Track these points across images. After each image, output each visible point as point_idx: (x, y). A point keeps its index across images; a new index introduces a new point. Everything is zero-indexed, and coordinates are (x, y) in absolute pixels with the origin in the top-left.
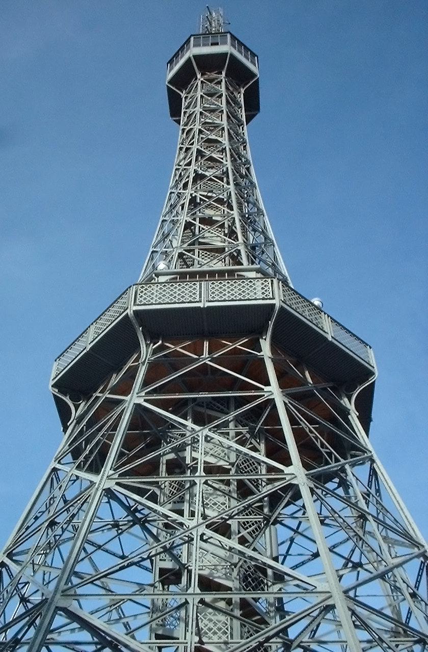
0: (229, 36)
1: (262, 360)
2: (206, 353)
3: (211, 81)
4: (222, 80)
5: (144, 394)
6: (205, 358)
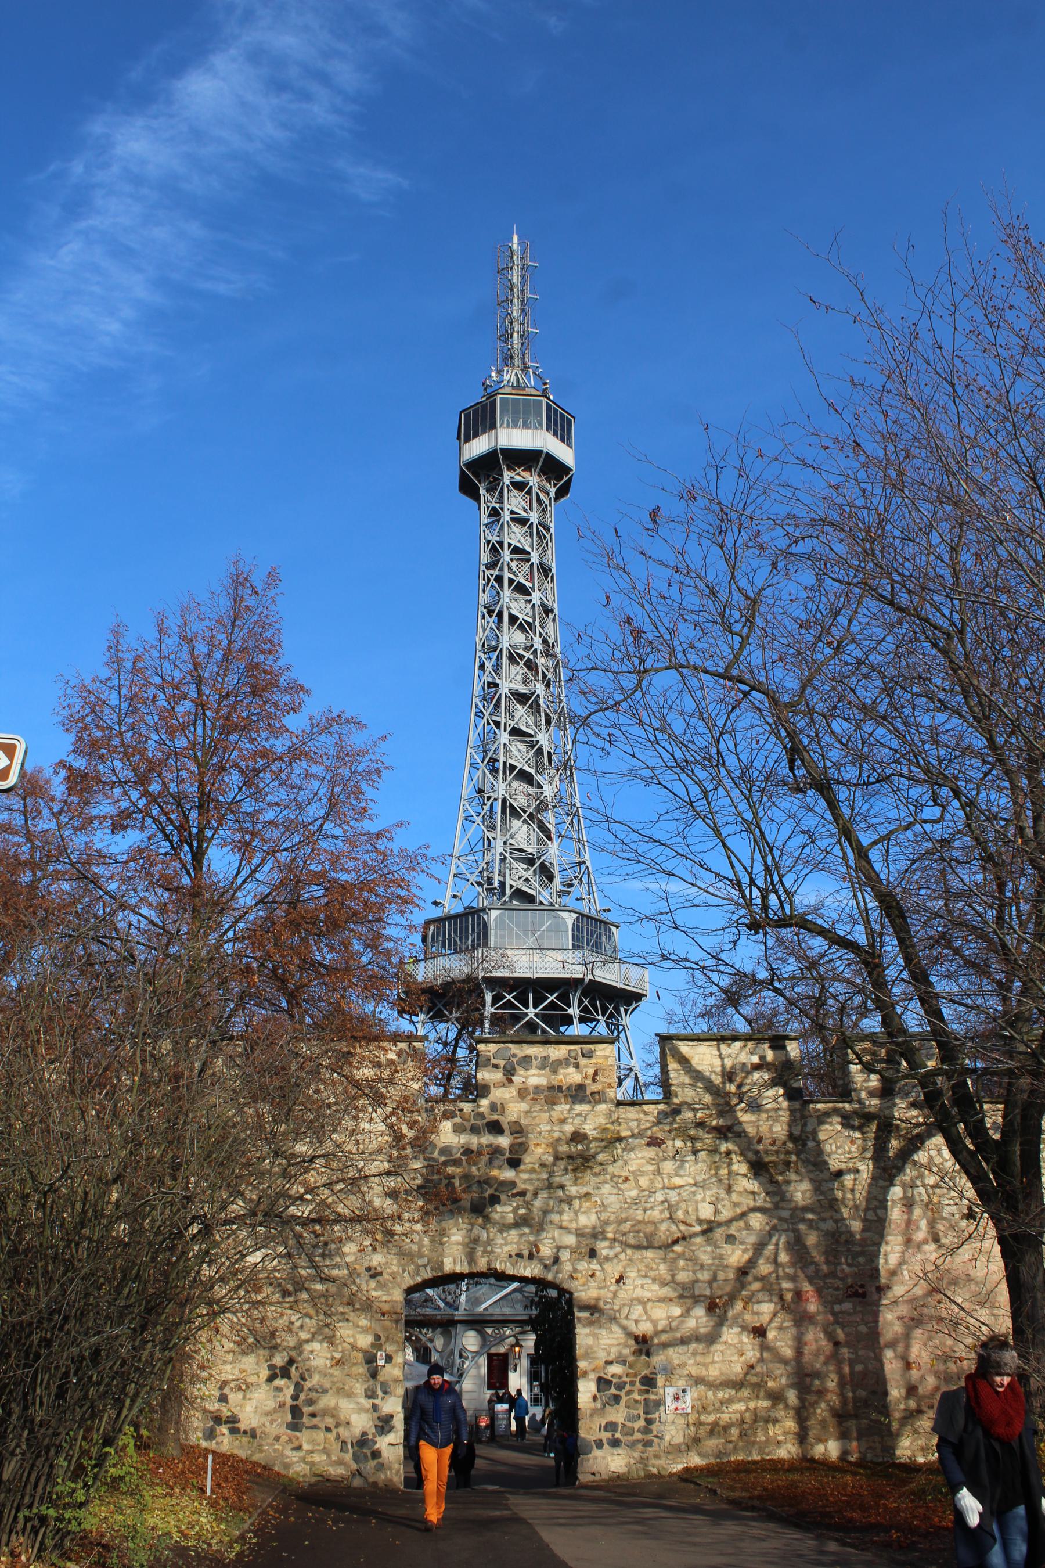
2: (531, 1012)
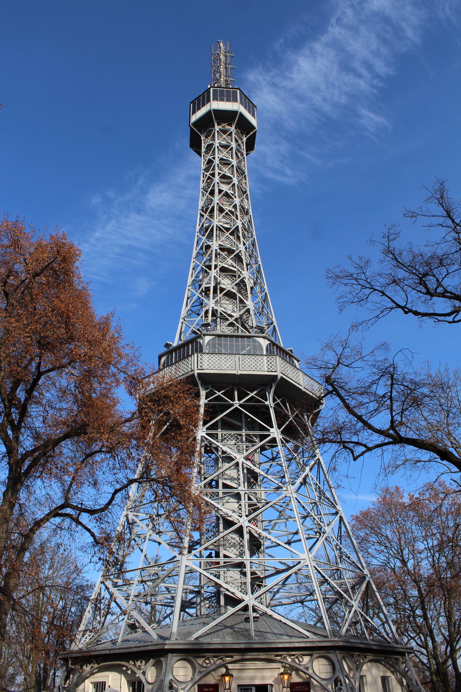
0: (238, 91)
1: (267, 407)
3: (224, 132)
4: (231, 132)
5: (205, 430)
6: (236, 404)
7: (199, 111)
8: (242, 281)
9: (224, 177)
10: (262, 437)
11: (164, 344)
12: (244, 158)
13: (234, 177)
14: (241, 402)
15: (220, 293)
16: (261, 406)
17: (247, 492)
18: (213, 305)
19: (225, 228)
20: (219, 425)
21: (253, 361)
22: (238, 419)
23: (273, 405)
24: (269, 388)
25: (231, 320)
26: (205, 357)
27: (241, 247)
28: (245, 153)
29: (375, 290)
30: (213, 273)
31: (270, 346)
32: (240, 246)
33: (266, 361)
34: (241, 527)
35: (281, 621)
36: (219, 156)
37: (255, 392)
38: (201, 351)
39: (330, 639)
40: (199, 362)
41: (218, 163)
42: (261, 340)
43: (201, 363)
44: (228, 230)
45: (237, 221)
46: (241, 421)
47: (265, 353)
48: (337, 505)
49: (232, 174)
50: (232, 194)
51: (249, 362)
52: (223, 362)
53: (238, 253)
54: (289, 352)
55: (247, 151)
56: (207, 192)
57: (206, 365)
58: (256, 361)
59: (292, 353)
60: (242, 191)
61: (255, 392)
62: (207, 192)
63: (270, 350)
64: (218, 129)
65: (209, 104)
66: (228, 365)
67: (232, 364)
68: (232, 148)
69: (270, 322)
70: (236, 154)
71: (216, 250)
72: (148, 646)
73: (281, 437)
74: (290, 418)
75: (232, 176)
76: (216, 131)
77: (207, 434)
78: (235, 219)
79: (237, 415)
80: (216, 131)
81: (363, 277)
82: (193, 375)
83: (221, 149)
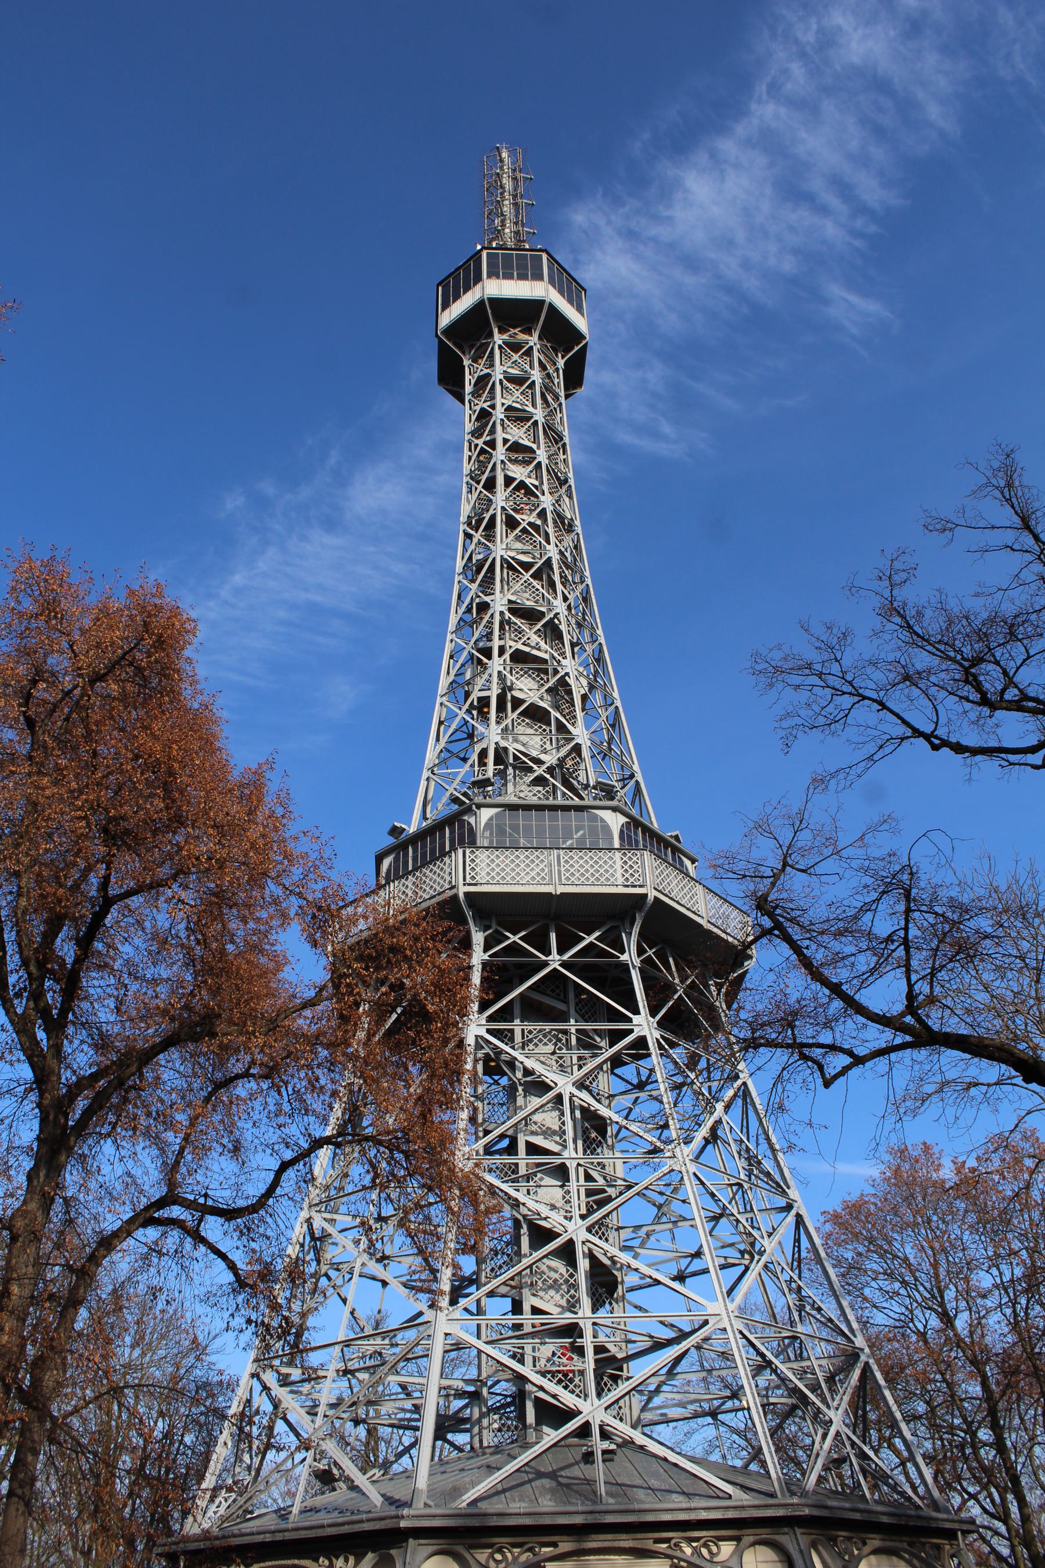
0: (545, 256)
1: (625, 968)
3: (515, 347)
4: (531, 348)
5: (484, 1022)
6: (555, 960)
7: (458, 302)
8: (563, 682)
9: (515, 447)
10: (615, 1037)
11: (389, 828)
12: (560, 405)
13: (539, 448)
14: (565, 957)
15: (513, 711)
16: (609, 965)
17: (581, 1162)
18: (498, 738)
19: (522, 564)
20: (517, 1010)
21: (591, 862)
22: (559, 995)
23: (637, 962)
24: (627, 924)
25: (539, 771)
26: (482, 856)
27: (559, 606)
28: (562, 394)
29: (864, 698)
30: (496, 664)
31: (628, 829)
32: (555, 603)
33: (619, 863)
34: (571, 1243)
35: (665, 1459)
36: (504, 401)
37: (597, 934)
38: (473, 843)
39: (780, 1499)
40: (468, 868)
41: (502, 416)
42: (607, 816)
43: (473, 869)
44: (526, 566)
45: (548, 547)
46: (565, 1001)
47: (617, 845)
48: (789, 1188)
49: (534, 442)
50: (536, 487)
51: (582, 866)
52: (522, 866)
53: (552, 620)
54: (673, 841)
55: (566, 389)
56: (478, 483)
57: (483, 874)
58: (596, 862)
59: (679, 842)
60: (558, 478)
61: (597, 934)
62: (478, 483)
63: (630, 837)
64: (500, 342)
65: (479, 286)
66: (533, 874)
67: (543, 870)
68: (534, 382)
69: (627, 773)
70: (543, 396)
71: (502, 613)
72: (361, 1521)
73: (657, 1034)
74: (676, 991)
75: (534, 446)
76: (497, 347)
77: (488, 1031)
78: (543, 542)
79: (558, 987)
80: (497, 347)
81: (835, 668)
82: (455, 897)
83: (509, 385)
